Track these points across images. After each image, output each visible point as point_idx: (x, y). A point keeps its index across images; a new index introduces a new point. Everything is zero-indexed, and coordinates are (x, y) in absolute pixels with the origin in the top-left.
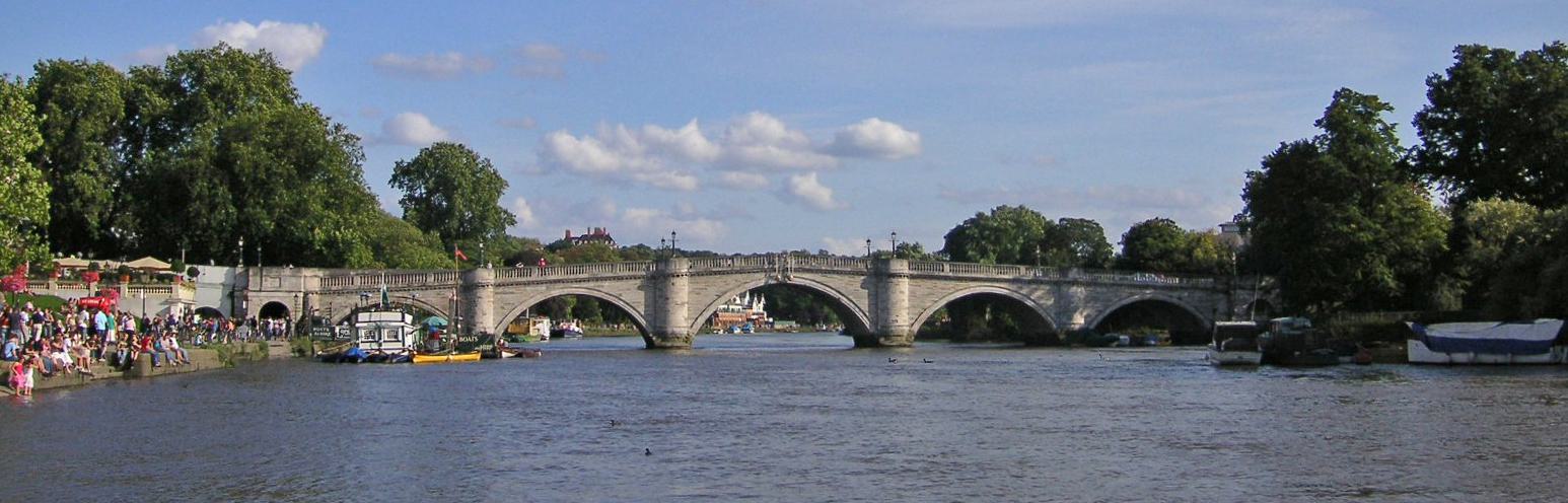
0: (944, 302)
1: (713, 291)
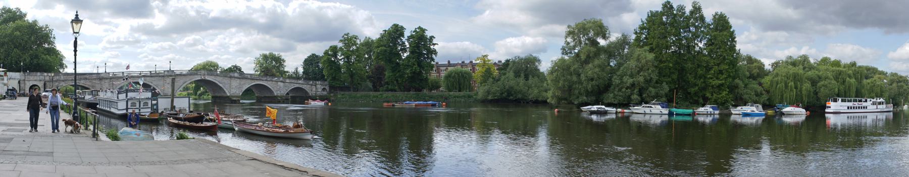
1: (182, 81)
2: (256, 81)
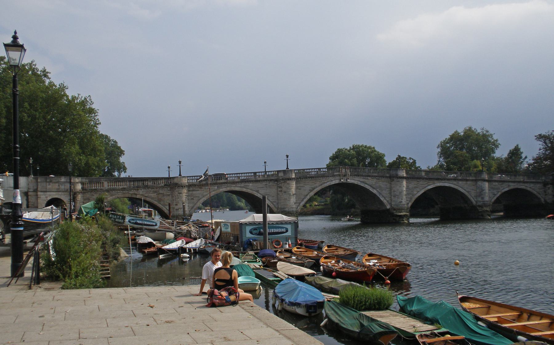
0: (422, 191)
1: (308, 187)
2: (436, 182)
